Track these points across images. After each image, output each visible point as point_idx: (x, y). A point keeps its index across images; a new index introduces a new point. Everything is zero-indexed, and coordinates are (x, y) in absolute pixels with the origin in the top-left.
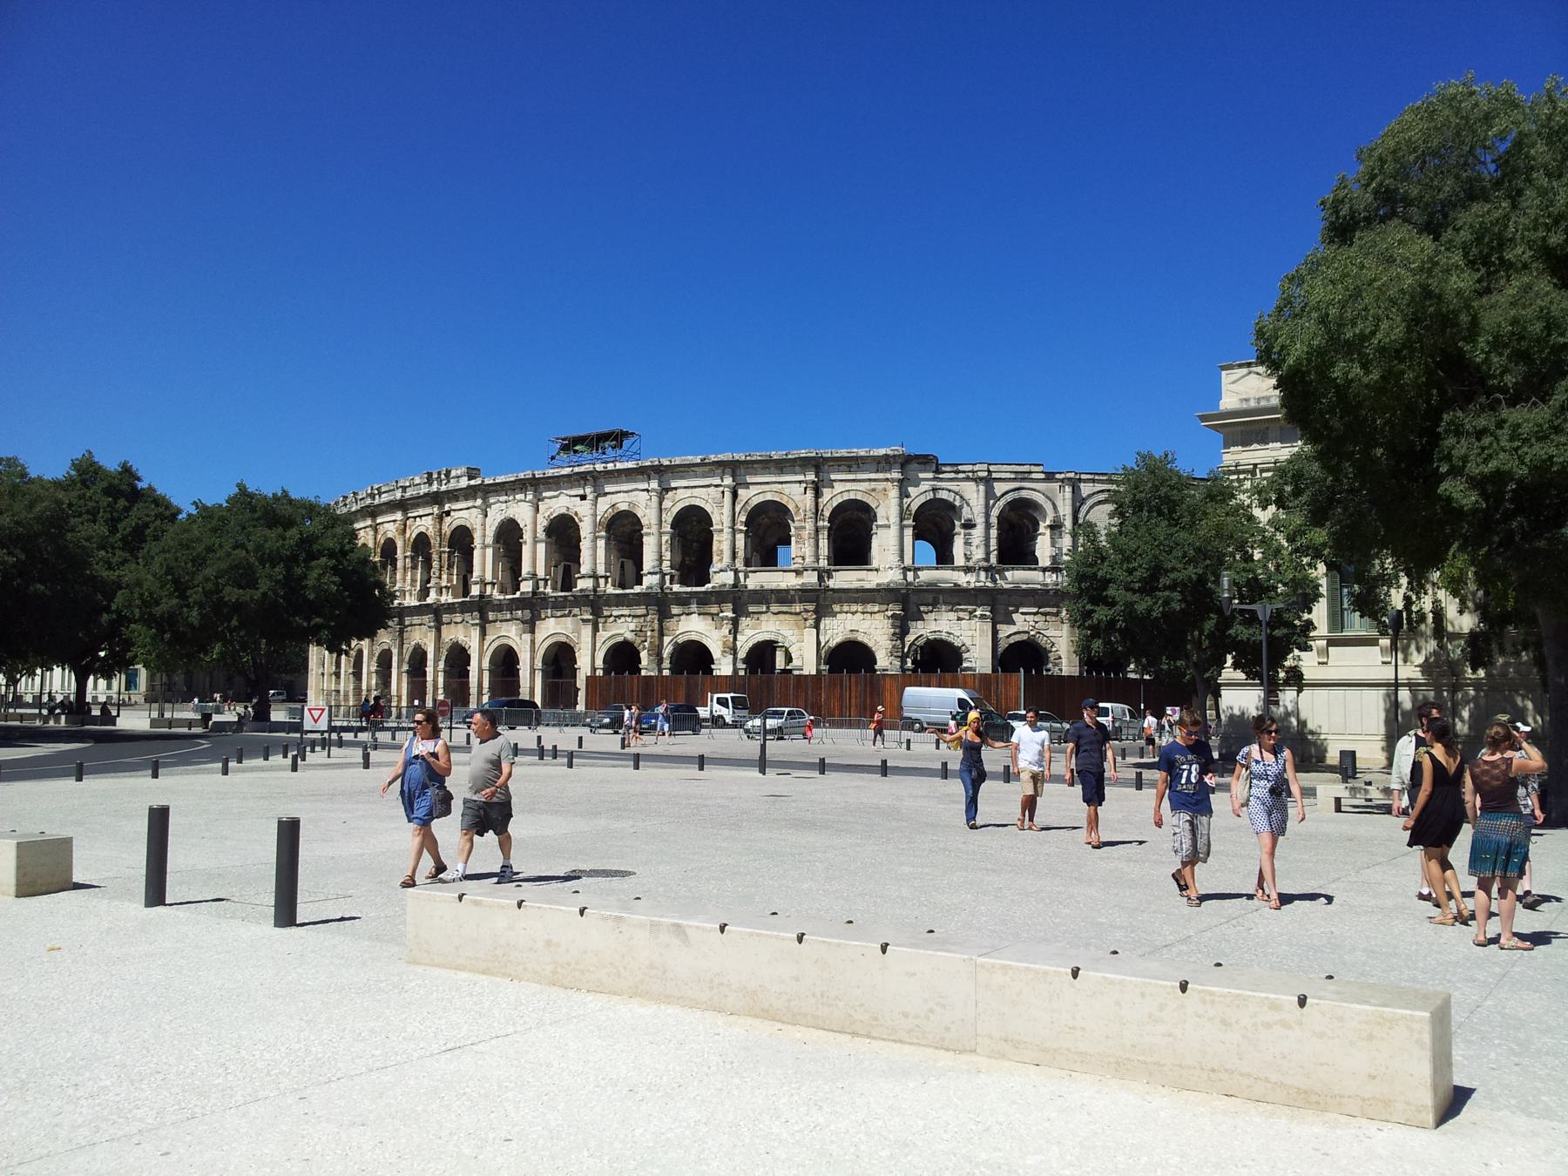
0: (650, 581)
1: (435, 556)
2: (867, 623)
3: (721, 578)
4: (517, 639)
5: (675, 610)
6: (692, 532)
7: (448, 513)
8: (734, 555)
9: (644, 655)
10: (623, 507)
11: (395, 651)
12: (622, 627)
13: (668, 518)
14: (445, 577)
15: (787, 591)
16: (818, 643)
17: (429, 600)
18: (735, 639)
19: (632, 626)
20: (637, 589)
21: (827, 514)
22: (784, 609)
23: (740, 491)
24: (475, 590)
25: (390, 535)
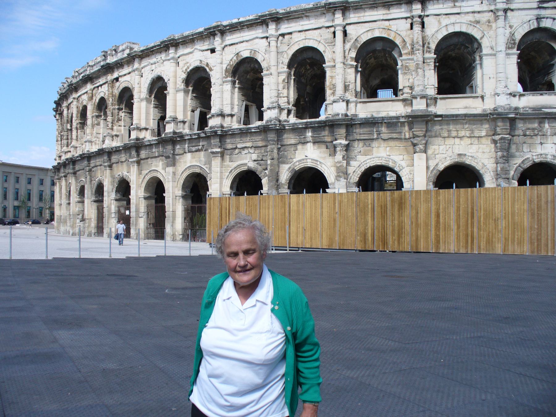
0: (269, 115)
1: (109, 113)
2: (474, 148)
3: (333, 108)
4: (163, 172)
5: (290, 139)
6: (308, 70)
7: (117, 79)
8: (346, 88)
9: (264, 181)
10: (246, 54)
11: (86, 186)
12: (247, 160)
13: (286, 59)
14: (115, 128)
15: (397, 118)
16: (428, 168)
17: (104, 146)
18: (348, 164)
19: (254, 157)
20: (259, 123)
21: (433, 46)
22: (395, 136)
23: (349, 29)
24: (134, 135)
25: (85, 103)
